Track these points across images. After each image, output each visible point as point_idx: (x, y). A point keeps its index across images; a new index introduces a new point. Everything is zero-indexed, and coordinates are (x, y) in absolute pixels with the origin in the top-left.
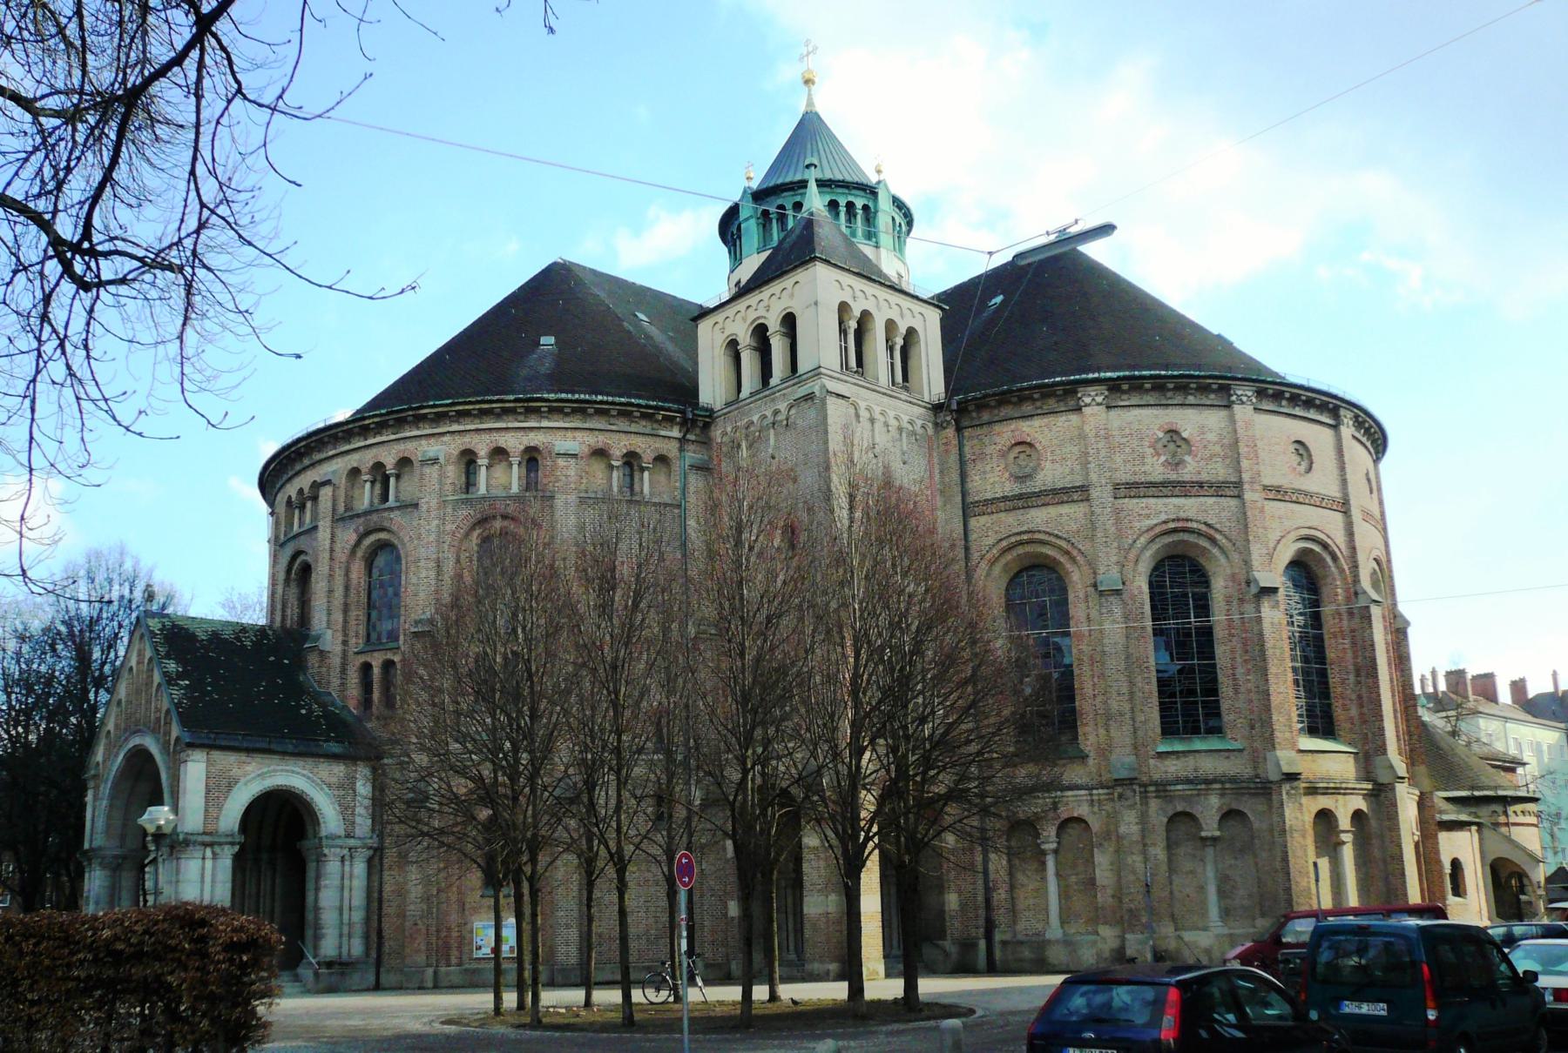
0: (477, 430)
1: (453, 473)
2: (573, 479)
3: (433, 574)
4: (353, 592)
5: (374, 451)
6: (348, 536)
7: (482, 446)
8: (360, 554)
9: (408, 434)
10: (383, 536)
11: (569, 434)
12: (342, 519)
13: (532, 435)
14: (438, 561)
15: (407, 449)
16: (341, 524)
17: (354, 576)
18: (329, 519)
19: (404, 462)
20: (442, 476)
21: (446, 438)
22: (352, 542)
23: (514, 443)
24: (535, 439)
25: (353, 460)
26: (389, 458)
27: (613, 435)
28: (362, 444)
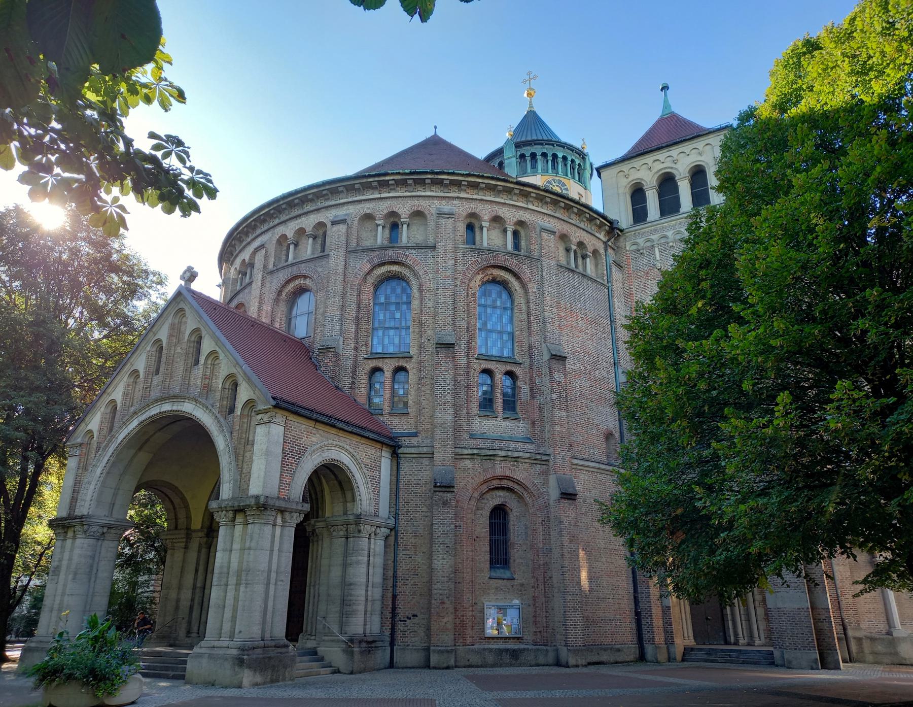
0: (482, 200)
1: (462, 227)
2: (553, 250)
3: (450, 301)
4: (363, 310)
5: (389, 202)
6: (362, 265)
7: (486, 212)
8: (371, 280)
9: (423, 194)
10: (395, 268)
11: (546, 218)
12: (355, 251)
13: (521, 212)
14: (454, 293)
15: (422, 205)
16: (353, 255)
17: (364, 297)
18: (342, 252)
19: (418, 214)
20: (455, 230)
21: (456, 202)
22: (366, 270)
23: (510, 216)
24: (526, 216)
25: (367, 208)
26: (404, 209)
27: (574, 228)
28: (378, 196)
